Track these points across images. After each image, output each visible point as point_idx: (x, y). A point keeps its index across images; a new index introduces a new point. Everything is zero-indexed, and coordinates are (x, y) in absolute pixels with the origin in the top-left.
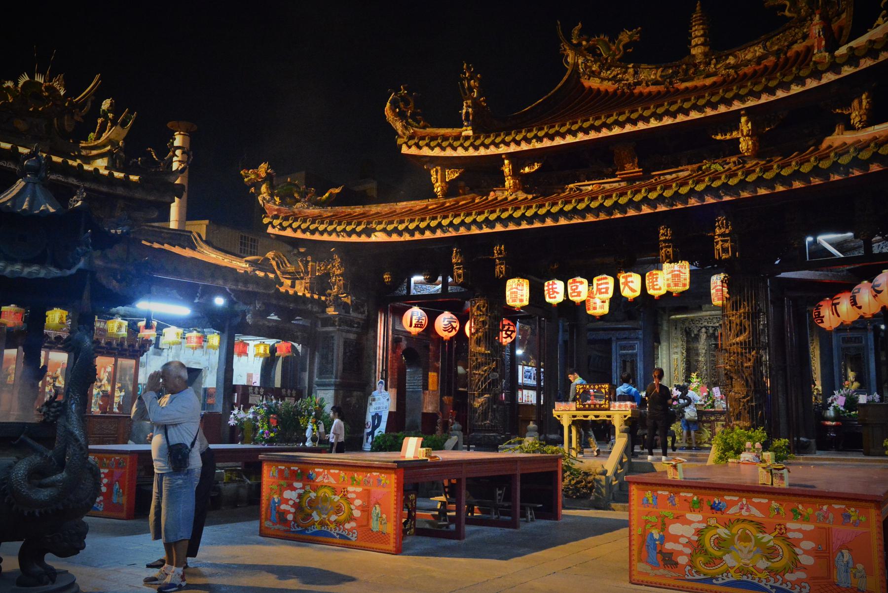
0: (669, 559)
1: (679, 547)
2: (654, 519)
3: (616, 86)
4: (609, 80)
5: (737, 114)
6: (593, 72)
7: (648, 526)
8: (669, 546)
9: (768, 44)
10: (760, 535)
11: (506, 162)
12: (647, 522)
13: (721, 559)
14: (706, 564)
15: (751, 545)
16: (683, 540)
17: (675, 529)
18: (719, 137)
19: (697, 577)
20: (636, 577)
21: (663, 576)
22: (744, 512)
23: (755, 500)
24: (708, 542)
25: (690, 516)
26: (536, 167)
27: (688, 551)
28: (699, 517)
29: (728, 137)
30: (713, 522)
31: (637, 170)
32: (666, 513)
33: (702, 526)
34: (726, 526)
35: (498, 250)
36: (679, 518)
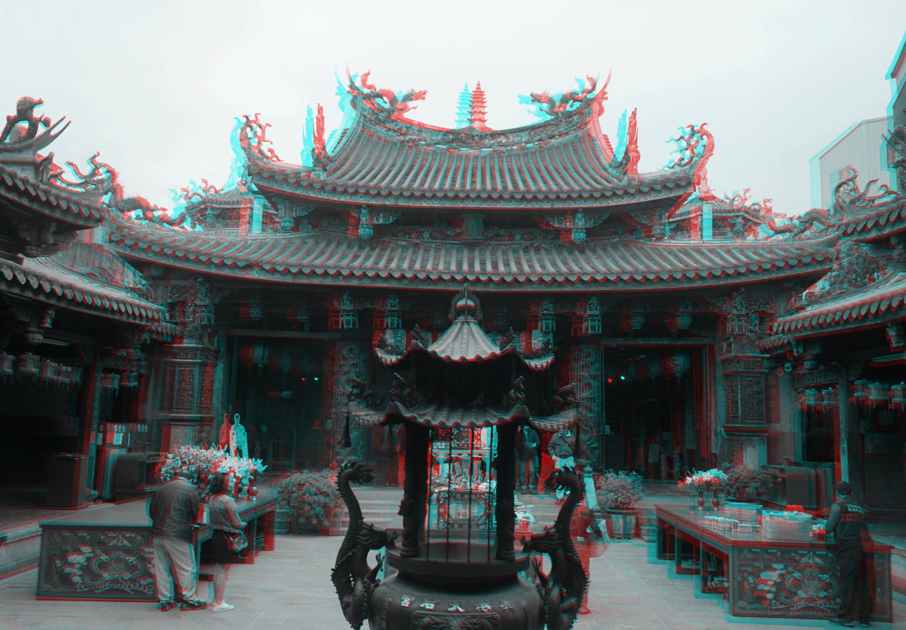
0: (760, 598)
1: (767, 588)
2: (750, 569)
3: (402, 138)
4: (394, 131)
5: (575, 211)
6: (379, 120)
7: (746, 574)
8: (761, 587)
9: (532, 133)
10: (821, 576)
11: (363, 211)
12: (745, 571)
13: (796, 594)
14: (786, 598)
15: (816, 582)
16: (771, 583)
17: (764, 575)
18: (556, 225)
19: (780, 607)
20: (738, 611)
21: (756, 609)
22: (811, 561)
23: (818, 553)
24: (789, 583)
25: (775, 566)
26: (391, 221)
27: (774, 589)
28: (782, 566)
29: (563, 226)
30: (790, 569)
31: (479, 237)
32: (756, 564)
33: (783, 572)
34: (799, 571)
35: (392, 304)
36: (769, 568)
